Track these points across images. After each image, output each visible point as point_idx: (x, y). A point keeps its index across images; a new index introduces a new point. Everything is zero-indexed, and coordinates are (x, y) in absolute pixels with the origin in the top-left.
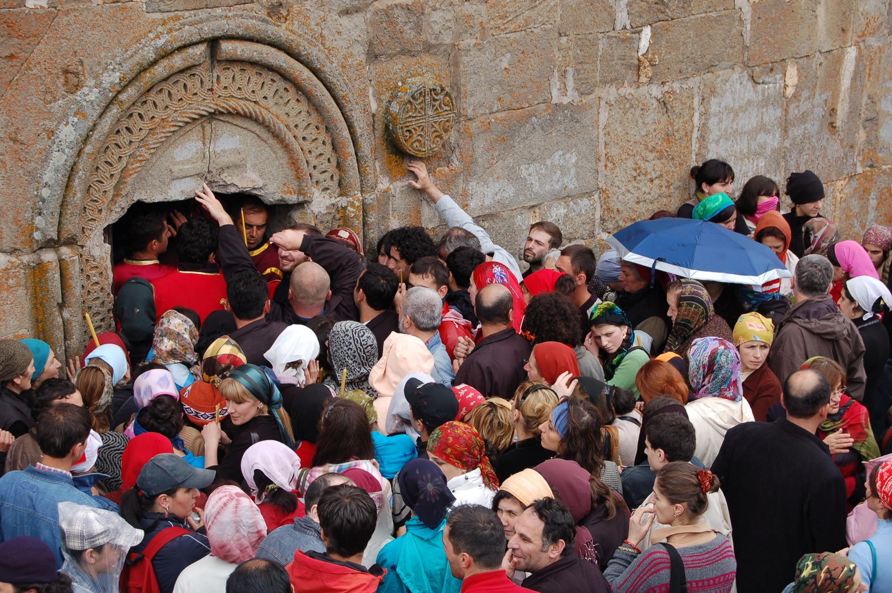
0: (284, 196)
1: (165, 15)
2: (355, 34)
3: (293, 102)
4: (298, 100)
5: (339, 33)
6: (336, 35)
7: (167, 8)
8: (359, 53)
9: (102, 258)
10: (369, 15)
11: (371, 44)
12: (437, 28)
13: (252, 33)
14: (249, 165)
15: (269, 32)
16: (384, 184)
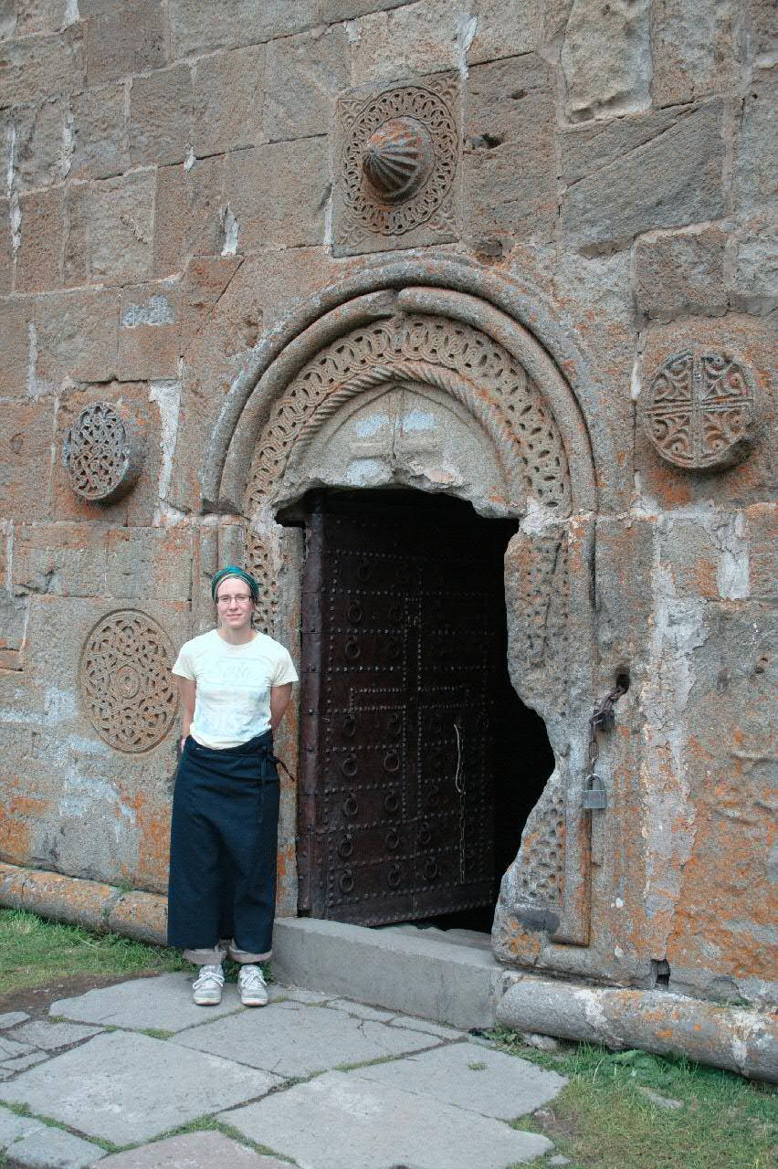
0: (491, 503)
1: (351, 259)
2: (608, 283)
3: (506, 374)
4: (512, 371)
5: (581, 280)
6: (576, 282)
7: (352, 251)
8: (617, 311)
9: (268, 538)
10: (632, 254)
11: (635, 299)
12: (749, 271)
13: (437, 275)
14: (446, 454)
15: (459, 274)
16: (645, 510)
